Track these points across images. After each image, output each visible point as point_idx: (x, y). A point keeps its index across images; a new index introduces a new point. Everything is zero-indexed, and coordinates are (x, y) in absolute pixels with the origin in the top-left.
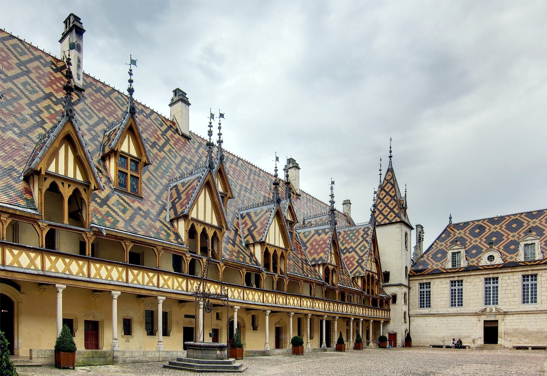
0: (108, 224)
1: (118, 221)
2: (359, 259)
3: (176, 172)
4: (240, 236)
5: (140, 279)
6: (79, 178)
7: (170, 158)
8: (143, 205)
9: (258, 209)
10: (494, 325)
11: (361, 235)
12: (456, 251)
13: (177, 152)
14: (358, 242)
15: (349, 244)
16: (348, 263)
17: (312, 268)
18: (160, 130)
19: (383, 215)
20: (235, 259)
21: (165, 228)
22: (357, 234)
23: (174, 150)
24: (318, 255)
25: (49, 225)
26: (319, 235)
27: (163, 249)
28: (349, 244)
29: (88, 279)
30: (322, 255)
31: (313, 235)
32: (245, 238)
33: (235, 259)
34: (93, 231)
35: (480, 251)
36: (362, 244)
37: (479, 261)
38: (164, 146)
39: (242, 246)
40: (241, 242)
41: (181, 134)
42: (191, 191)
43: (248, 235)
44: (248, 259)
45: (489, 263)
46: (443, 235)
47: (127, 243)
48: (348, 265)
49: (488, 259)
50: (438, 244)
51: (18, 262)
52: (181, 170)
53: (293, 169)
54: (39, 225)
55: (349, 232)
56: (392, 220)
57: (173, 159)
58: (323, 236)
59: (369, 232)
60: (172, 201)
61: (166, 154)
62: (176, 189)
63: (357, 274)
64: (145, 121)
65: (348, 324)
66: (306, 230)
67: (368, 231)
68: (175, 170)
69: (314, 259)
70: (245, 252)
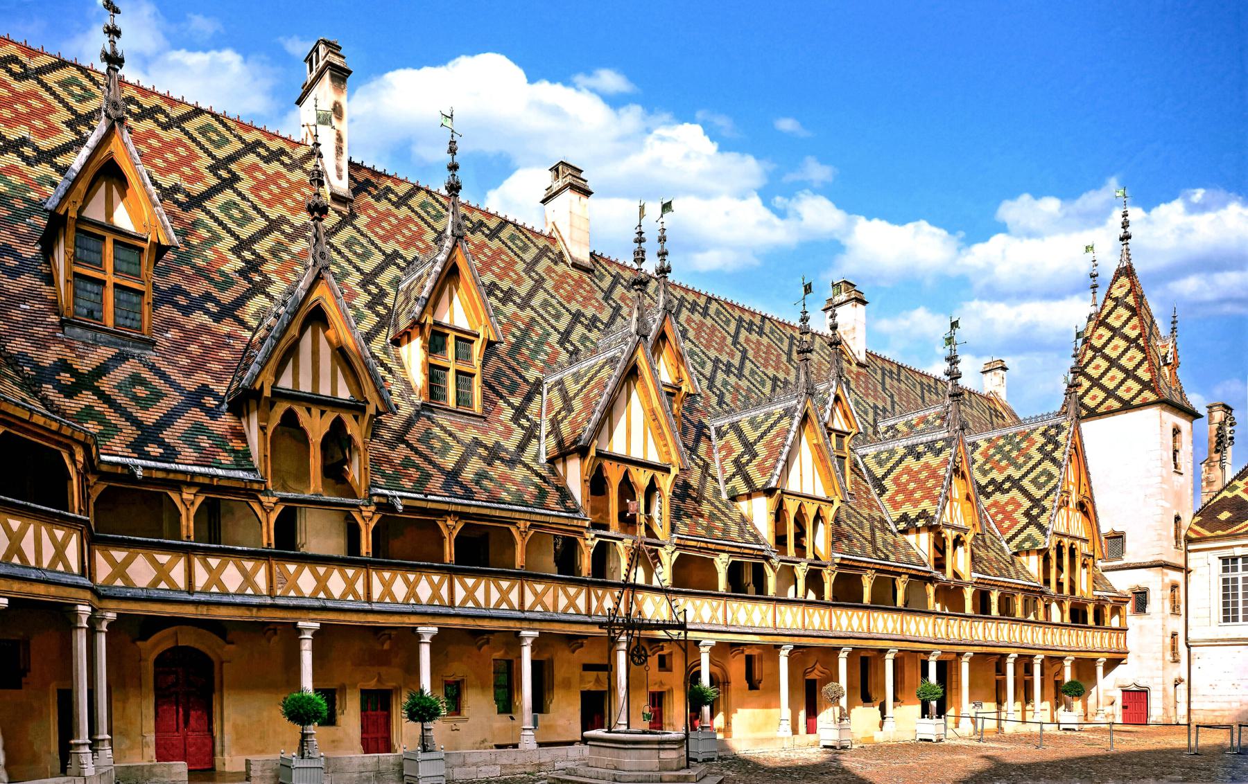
0: (409, 485)
1: (431, 476)
2: (1031, 508)
3: (561, 350)
4: (713, 478)
5: (481, 595)
6: (344, 393)
7: (546, 320)
8: (485, 433)
9: (760, 414)
13: (562, 305)
15: (1001, 470)
18: (522, 259)
20: (703, 532)
21: (537, 480)
22: (1024, 445)
23: (554, 302)
25: (282, 500)
26: (918, 457)
27: (532, 526)
28: (1001, 470)
29: (367, 606)
30: (926, 504)
32: (726, 482)
33: (703, 532)
34: (376, 504)
36: (1039, 469)
38: (531, 295)
39: (721, 502)
40: (717, 492)
41: (570, 261)
42: (596, 391)
43: (734, 475)
44: (734, 530)
47: (449, 522)
51: (220, 584)
52: (572, 344)
53: (849, 305)
54: (261, 503)
57: (552, 321)
58: (929, 458)
60: (550, 416)
61: (536, 312)
62: (560, 390)
63: (1027, 545)
64: (488, 247)
65: (1001, 670)
68: (557, 346)
70: (726, 515)
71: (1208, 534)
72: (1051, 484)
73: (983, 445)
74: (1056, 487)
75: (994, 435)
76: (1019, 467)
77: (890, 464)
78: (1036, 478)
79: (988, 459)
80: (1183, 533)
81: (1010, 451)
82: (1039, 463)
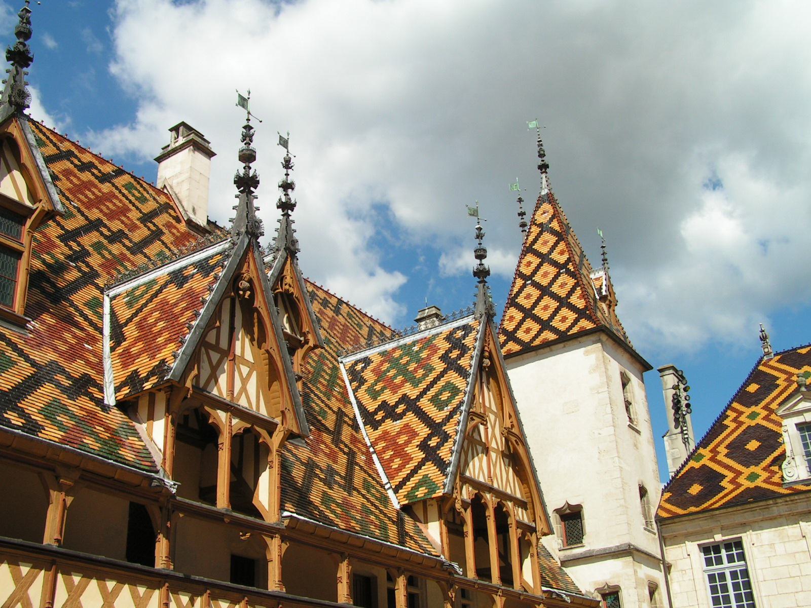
2: (429, 437)
11: (441, 352)
14: (430, 378)
19: (537, 319)
22: (424, 355)
24: (153, 357)
28: (395, 389)
31: (160, 291)
36: (441, 383)
46: (753, 388)
48: (386, 465)
50: (740, 413)
56: (570, 328)
58: (198, 283)
59: (468, 341)
67: (464, 337)
69: (133, 380)
71: (680, 511)
72: (455, 402)
74: (461, 403)
76: (415, 383)
79: (380, 375)
80: (653, 511)
81: (408, 363)
82: (442, 374)
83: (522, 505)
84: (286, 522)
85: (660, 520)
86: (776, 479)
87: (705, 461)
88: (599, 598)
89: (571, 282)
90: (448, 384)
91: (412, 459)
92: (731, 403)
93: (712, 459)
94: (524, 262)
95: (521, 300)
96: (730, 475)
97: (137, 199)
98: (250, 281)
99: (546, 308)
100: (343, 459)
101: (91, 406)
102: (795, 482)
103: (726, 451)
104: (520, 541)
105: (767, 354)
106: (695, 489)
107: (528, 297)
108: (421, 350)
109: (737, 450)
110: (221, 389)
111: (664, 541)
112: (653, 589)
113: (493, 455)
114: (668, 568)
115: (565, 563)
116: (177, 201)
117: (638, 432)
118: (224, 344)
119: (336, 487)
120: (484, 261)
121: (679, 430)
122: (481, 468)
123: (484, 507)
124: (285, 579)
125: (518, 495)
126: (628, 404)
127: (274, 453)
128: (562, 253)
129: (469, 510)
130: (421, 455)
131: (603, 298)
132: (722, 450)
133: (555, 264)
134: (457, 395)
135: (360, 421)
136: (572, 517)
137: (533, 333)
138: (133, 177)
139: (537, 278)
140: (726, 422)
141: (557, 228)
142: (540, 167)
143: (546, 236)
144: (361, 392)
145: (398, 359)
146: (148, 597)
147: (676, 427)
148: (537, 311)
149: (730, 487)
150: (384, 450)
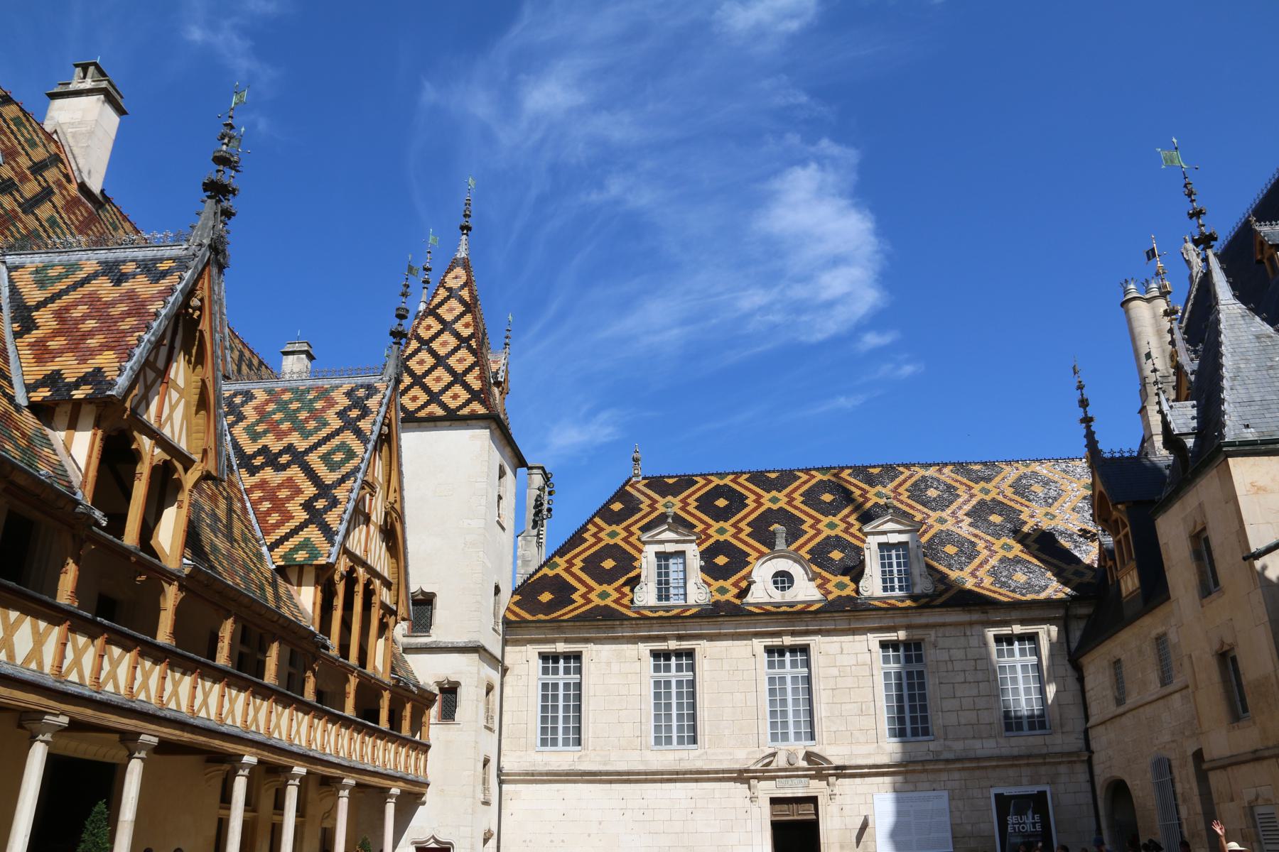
2: (315, 498)
10: (804, 813)
11: (339, 408)
12: (670, 548)
14: (323, 433)
16: (266, 505)
17: (29, 421)
19: (426, 389)
22: (319, 405)
24: (83, 361)
26: (119, 279)
28: (280, 435)
31: (86, 280)
35: (739, 560)
36: (336, 441)
37: (743, 593)
45: (778, 596)
46: (617, 506)
48: (262, 517)
49: (775, 582)
50: (601, 530)
55: (286, 397)
59: (372, 403)
66: (56, 258)
67: (368, 397)
69: (53, 380)
72: (349, 466)
73: (261, 396)
74: (357, 469)
75: (278, 386)
76: (306, 435)
77: (61, 286)
78: (329, 453)
79: (263, 415)
80: (502, 611)
81: (298, 410)
82: (337, 432)
83: (388, 584)
84: (187, 571)
85: (507, 622)
86: (625, 601)
87: (559, 571)
88: (437, 691)
89: (471, 359)
90: (343, 443)
91: (293, 518)
92: (594, 517)
93: (567, 570)
94: (424, 324)
95: (412, 364)
96: (583, 590)
97: (27, 140)
98: (202, 300)
99: (438, 379)
100: (223, 504)
101: (5, 402)
102: (644, 607)
103: (582, 564)
104: (381, 620)
105: (637, 475)
106: (546, 597)
107: (421, 362)
108: (316, 399)
109: (592, 566)
110: (151, 416)
111: (505, 643)
112: (490, 689)
113: (372, 527)
114: (505, 671)
115: (407, 650)
116: (70, 156)
117: (503, 529)
118: (161, 364)
119: (220, 535)
120: (404, 322)
121: (535, 532)
122: (359, 540)
123: (356, 580)
124: (176, 632)
125: (386, 575)
126: (500, 498)
127: (187, 492)
128: (467, 326)
129: (343, 582)
130: (304, 516)
131: (498, 384)
132: (578, 563)
133: (457, 335)
134: (352, 458)
135: (235, 462)
136: (425, 602)
137: (420, 403)
138: (22, 110)
139: (434, 345)
140: (586, 535)
141: (467, 298)
142: (462, 228)
143: (454, 303)
144: (238, 430)
145: (286, 403)
146: (47, 633)
147: (534, 528)
148: (428, 381)
149: (581, 601)
150: (261, 500)
